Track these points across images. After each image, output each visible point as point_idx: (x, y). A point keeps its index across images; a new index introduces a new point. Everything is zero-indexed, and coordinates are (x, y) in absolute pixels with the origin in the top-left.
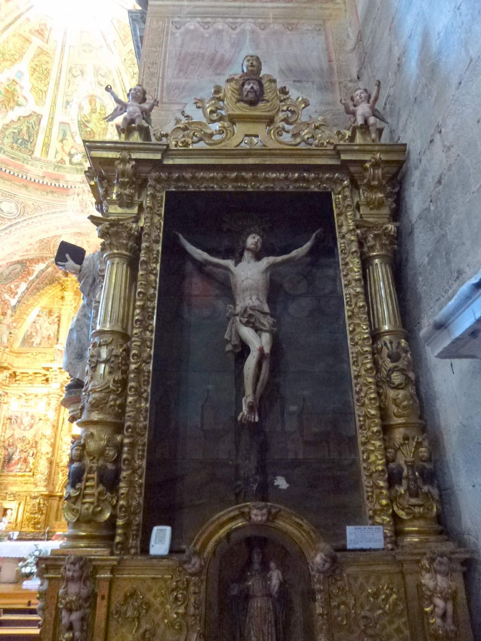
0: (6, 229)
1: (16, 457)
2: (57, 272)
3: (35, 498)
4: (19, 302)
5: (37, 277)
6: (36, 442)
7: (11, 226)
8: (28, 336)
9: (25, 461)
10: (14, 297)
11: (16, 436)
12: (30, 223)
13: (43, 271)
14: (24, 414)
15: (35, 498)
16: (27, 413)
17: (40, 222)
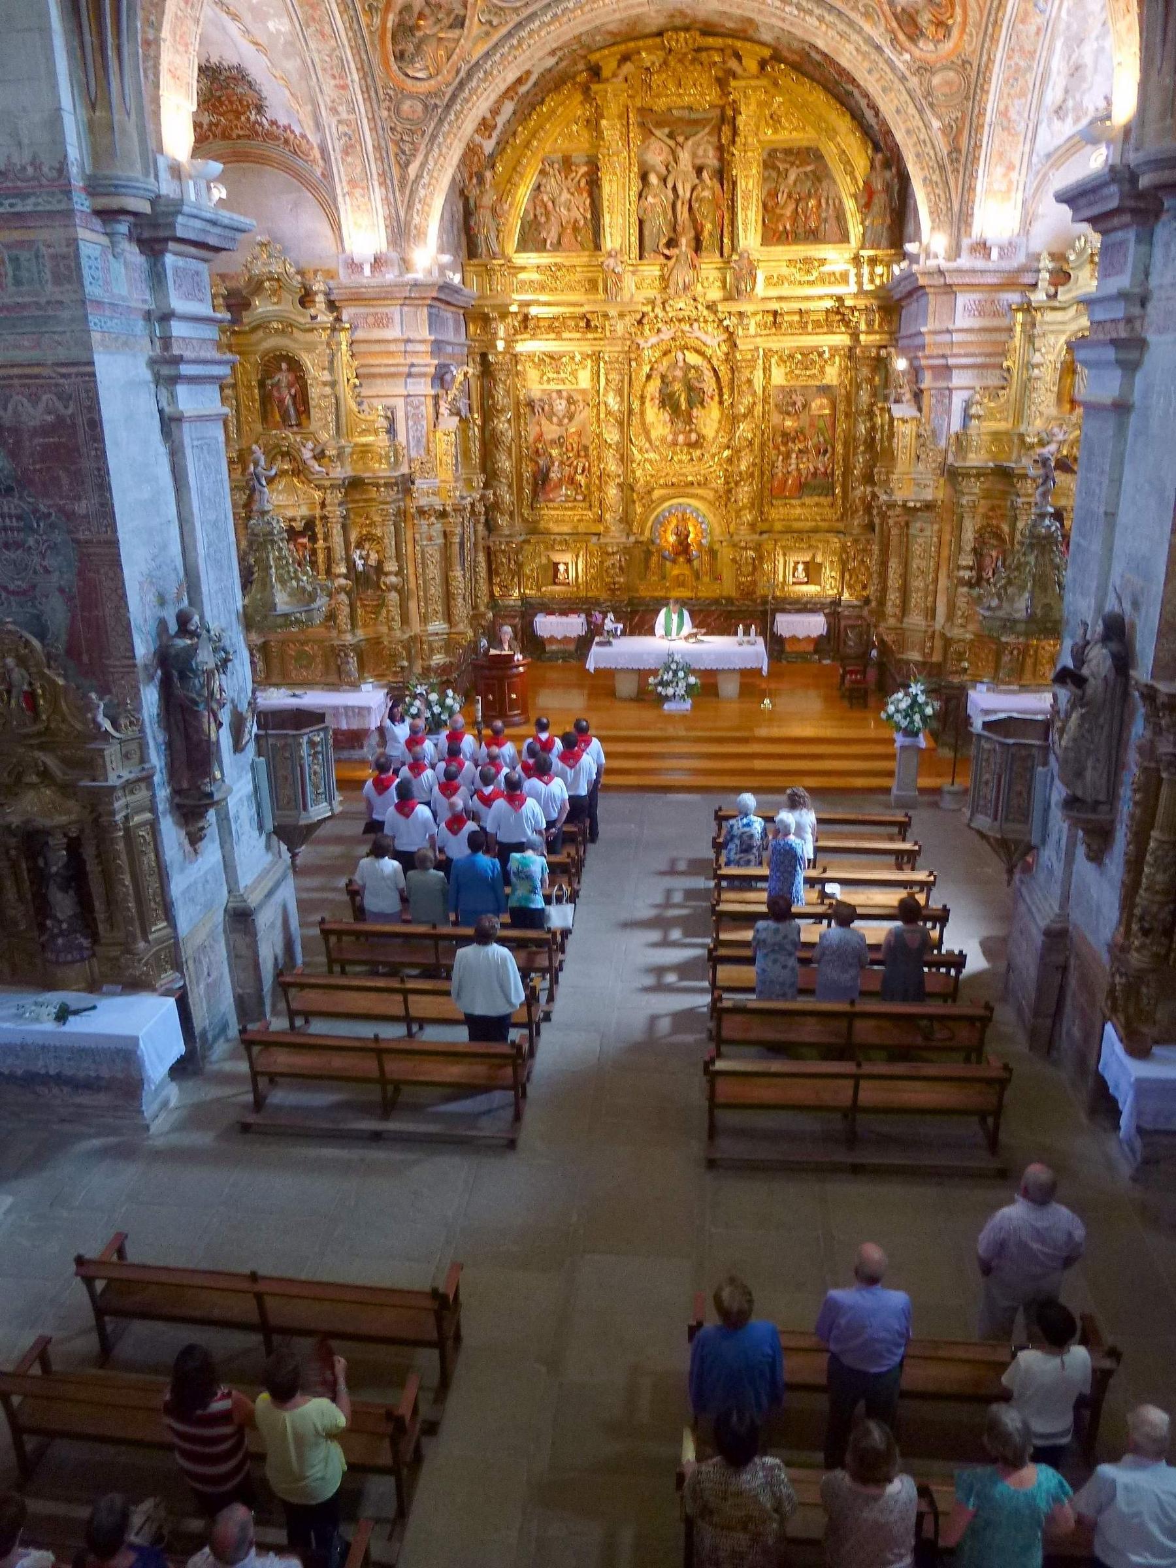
0: (510, 34)
1: (554, 475)
2: (575, 64)
3: (614, 554)
4: (498, 143)
5: (535, 85)
6: (586, 448)
7: (519, 25)
8: (530, 224)
9: (572, 481)
10: (490, 136)
11: (548, 437)
12: (559, 12)
13: (550, 70)
14: (554, 395)
15: (614, 554)
16: (559, 392)
17: (581, 8)
